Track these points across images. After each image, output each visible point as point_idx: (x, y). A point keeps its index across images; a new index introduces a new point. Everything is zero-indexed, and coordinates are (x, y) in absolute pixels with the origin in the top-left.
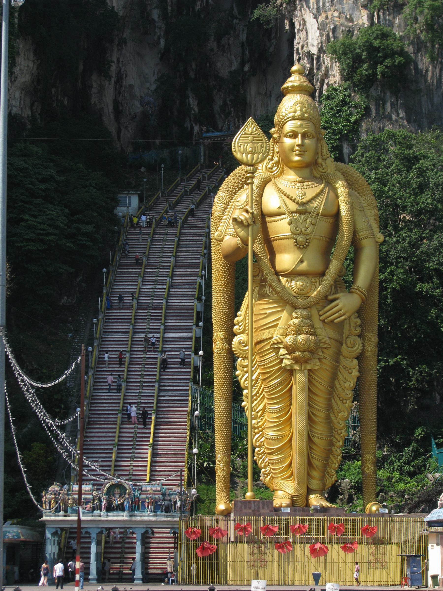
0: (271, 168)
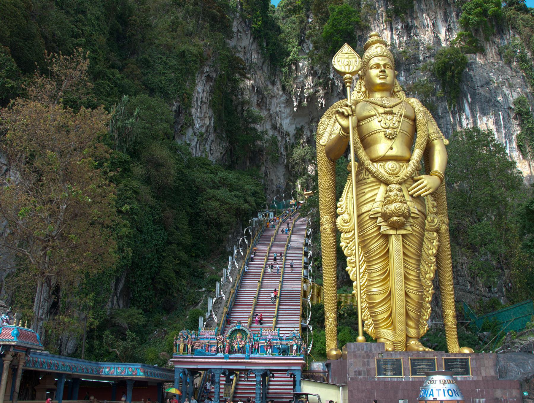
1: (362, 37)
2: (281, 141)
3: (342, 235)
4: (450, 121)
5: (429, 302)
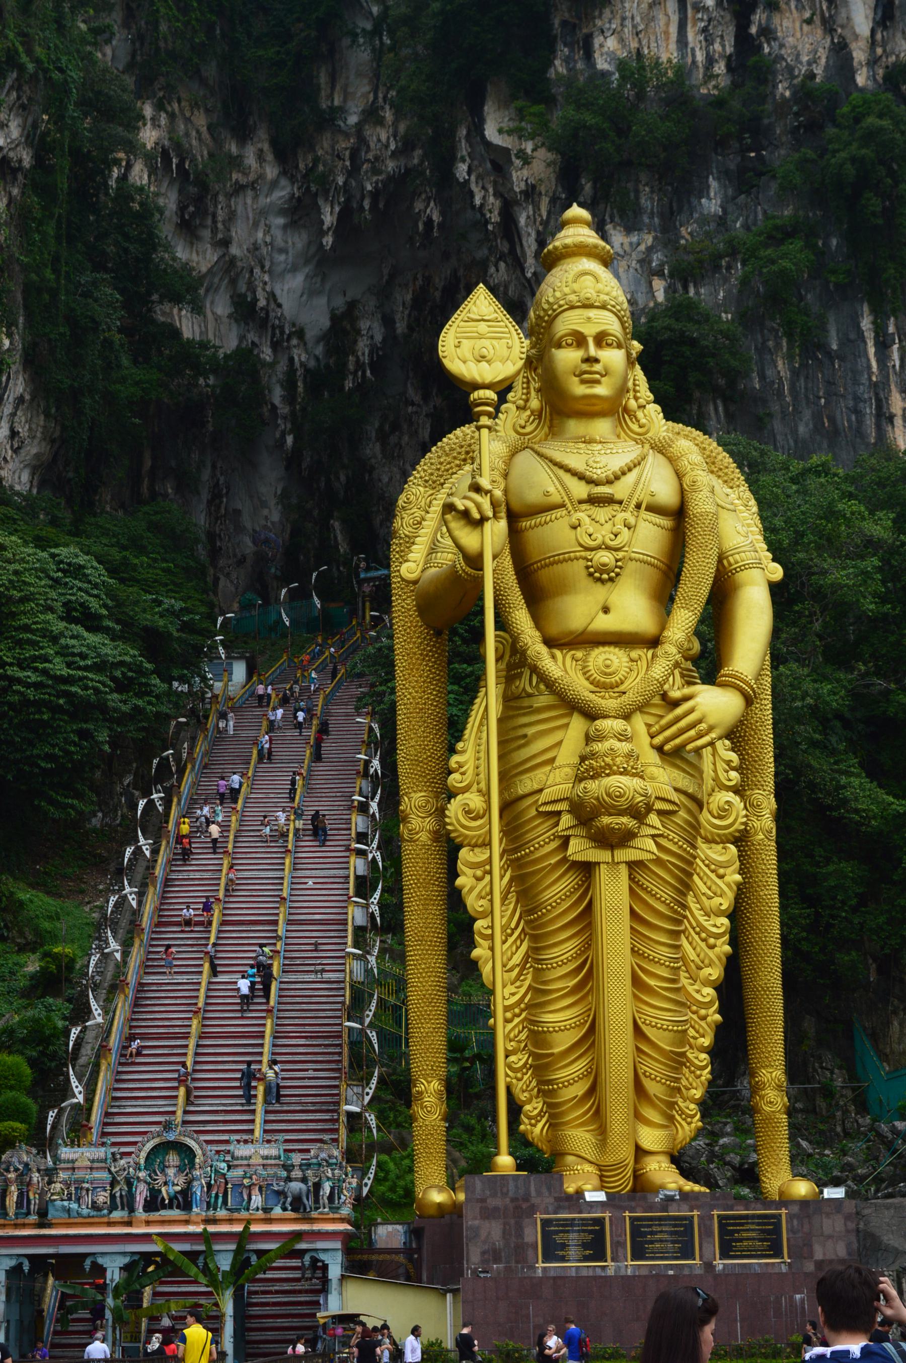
0: (524, 427)
1: (574, 26)
2: (272, 365)
3: (464, 853)
4: (870, 373)
5: (702, 1049)
